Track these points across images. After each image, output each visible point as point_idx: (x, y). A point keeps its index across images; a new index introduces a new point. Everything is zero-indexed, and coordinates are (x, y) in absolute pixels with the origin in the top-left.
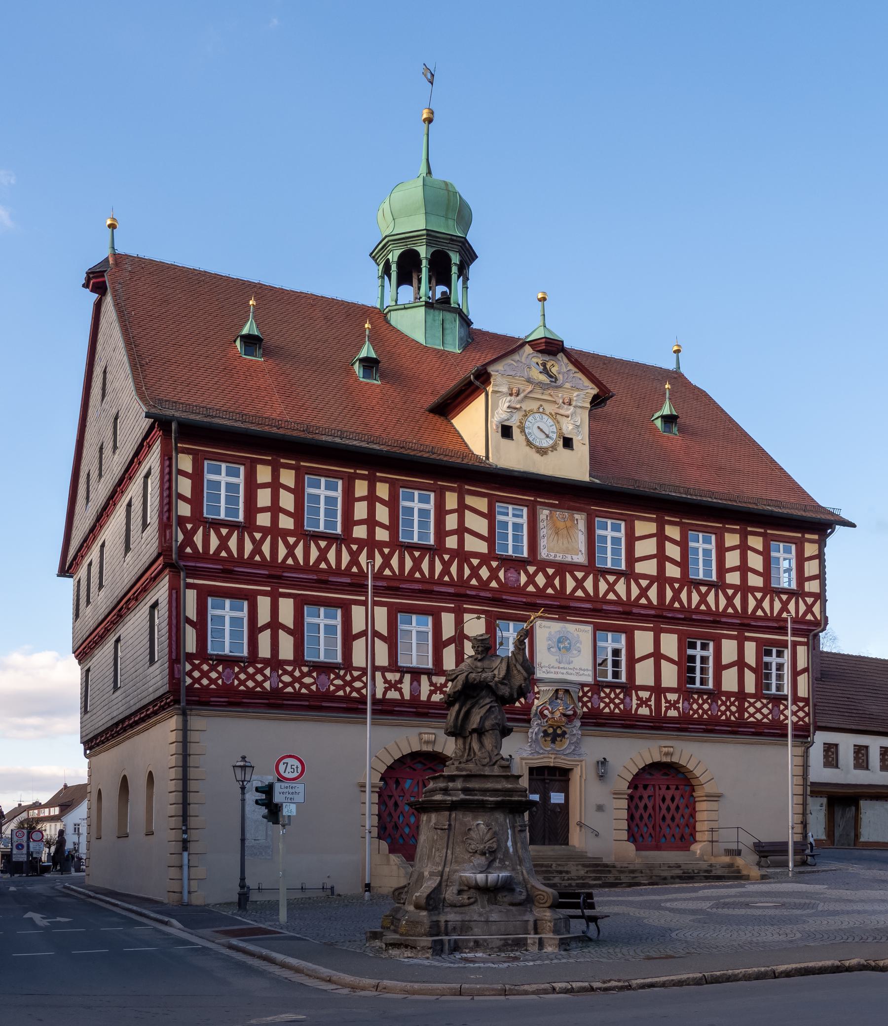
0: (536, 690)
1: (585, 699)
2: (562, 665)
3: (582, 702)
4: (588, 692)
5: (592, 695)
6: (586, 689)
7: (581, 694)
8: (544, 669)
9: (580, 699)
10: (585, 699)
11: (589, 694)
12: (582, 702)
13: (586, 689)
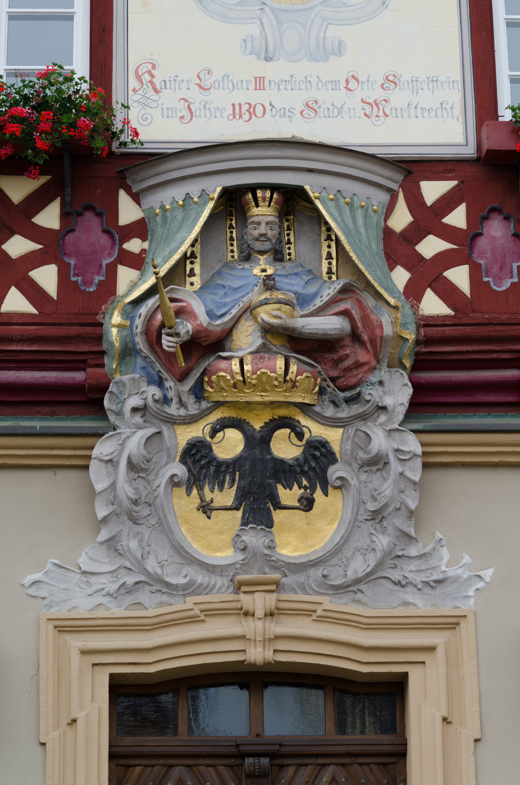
0: (128, 212)
1: (431, 246)
2: (273, 71)
3: (414, 262)
4: (447, 203)
5: (477, 219)
6: (432, 190)
7: (401, 219)
8: (169, 98)
9: (398, 248)
10: (431, 246)
11: (458, 218)
12: (414, 262)
13: (432, 190)
